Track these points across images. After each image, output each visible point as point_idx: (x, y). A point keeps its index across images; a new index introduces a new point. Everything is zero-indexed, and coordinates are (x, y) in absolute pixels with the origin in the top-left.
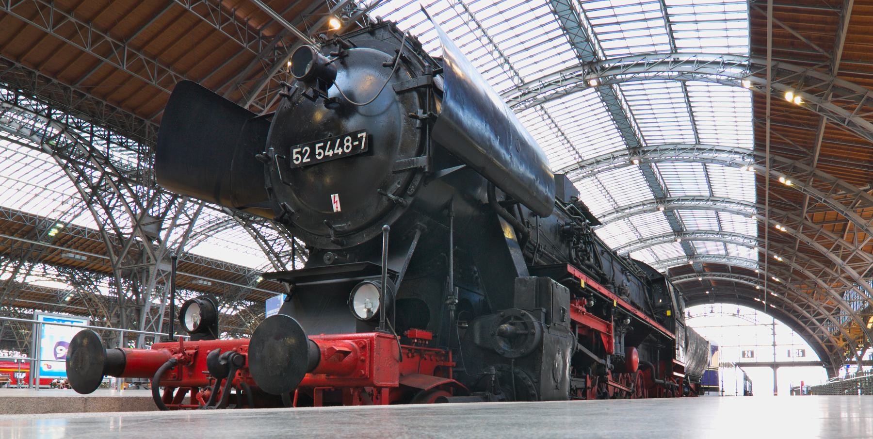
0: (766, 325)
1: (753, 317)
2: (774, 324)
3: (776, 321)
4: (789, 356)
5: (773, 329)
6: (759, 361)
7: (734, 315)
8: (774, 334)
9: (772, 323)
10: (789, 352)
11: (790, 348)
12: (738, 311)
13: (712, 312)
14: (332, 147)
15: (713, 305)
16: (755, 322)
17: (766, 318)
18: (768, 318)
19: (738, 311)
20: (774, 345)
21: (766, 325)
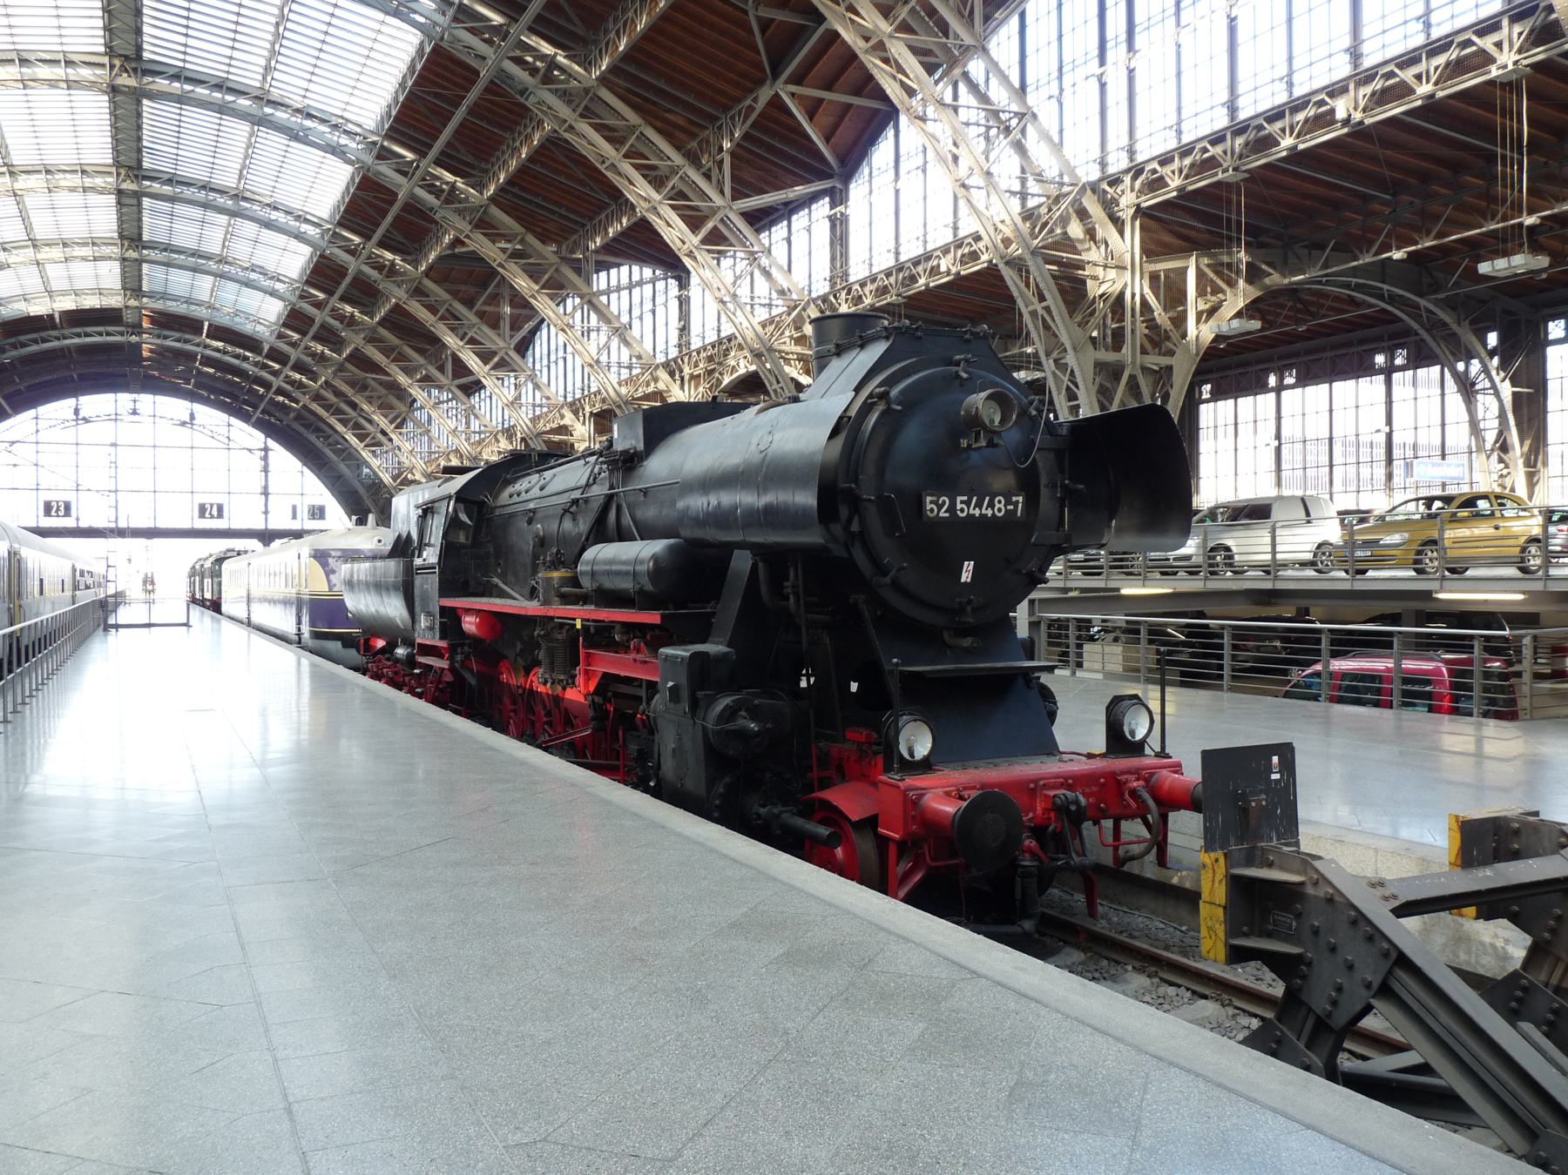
0: (250, 450)
1: (224, 430)
2: (266, 449)
3: (271, 443)
4: (294, 517)
5: (265, 458)
6: (236, 525)
7: (183, 424)
8: (266, 470)
9: (262, 446)
10: (294, 509)
11: (297, 501)
12: (192, 417)
13: (135, 412)
14: (979, 505)
15: (135, 396)
16: (226, 441)
17: (248, 435)
18: (256, 438)
19: (192, 417)
20: (266, 493)
21: (250, 450)
